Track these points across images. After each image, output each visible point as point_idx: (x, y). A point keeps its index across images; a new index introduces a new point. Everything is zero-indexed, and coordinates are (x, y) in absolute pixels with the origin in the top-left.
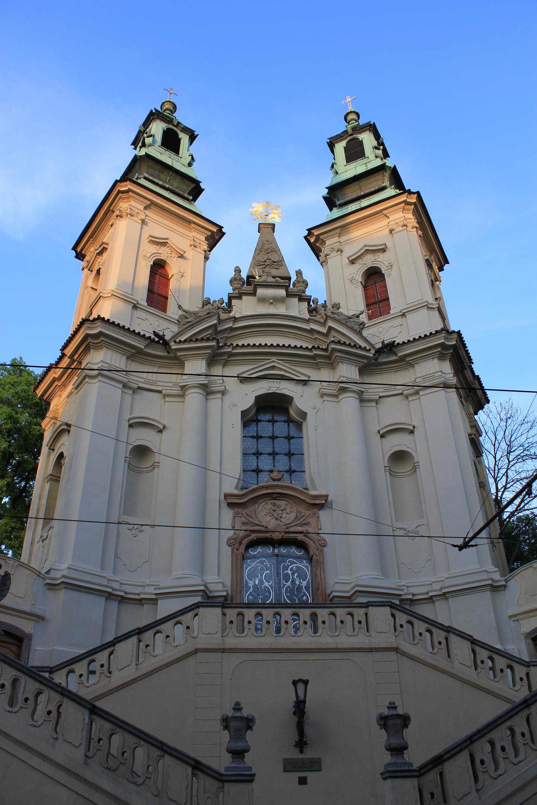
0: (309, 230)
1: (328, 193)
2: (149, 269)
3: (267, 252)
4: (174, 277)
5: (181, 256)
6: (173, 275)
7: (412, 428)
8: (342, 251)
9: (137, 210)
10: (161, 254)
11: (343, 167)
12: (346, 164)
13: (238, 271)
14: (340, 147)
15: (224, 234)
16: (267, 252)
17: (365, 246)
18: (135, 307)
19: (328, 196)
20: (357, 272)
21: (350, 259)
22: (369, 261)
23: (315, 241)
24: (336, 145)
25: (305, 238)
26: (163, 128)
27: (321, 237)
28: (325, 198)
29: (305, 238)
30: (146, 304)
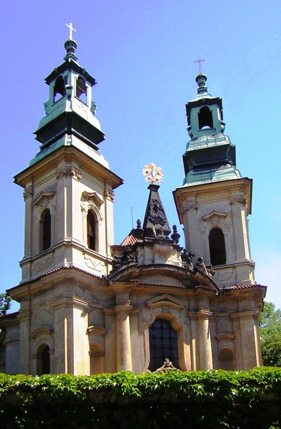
0: (177, 189)
1: (186, 154)
3: (154, 209)
7: (234, 338)
8: (197, 209)
11: (196, 131)
12: (198, 130)
13: (139, 222)
14: (195, 112)
15: (123, 183)
16: (154, 209)
17: (214, 211)
19: (186, 155)
20: (208, 227)
21: (204, 218)
22: (215, 222)
23: (179, 195)
24: (192, 109)
25: (174, 192)
27: (185, 195)
28: (183, 157)
29: (174, 192)
30: (87, 247)
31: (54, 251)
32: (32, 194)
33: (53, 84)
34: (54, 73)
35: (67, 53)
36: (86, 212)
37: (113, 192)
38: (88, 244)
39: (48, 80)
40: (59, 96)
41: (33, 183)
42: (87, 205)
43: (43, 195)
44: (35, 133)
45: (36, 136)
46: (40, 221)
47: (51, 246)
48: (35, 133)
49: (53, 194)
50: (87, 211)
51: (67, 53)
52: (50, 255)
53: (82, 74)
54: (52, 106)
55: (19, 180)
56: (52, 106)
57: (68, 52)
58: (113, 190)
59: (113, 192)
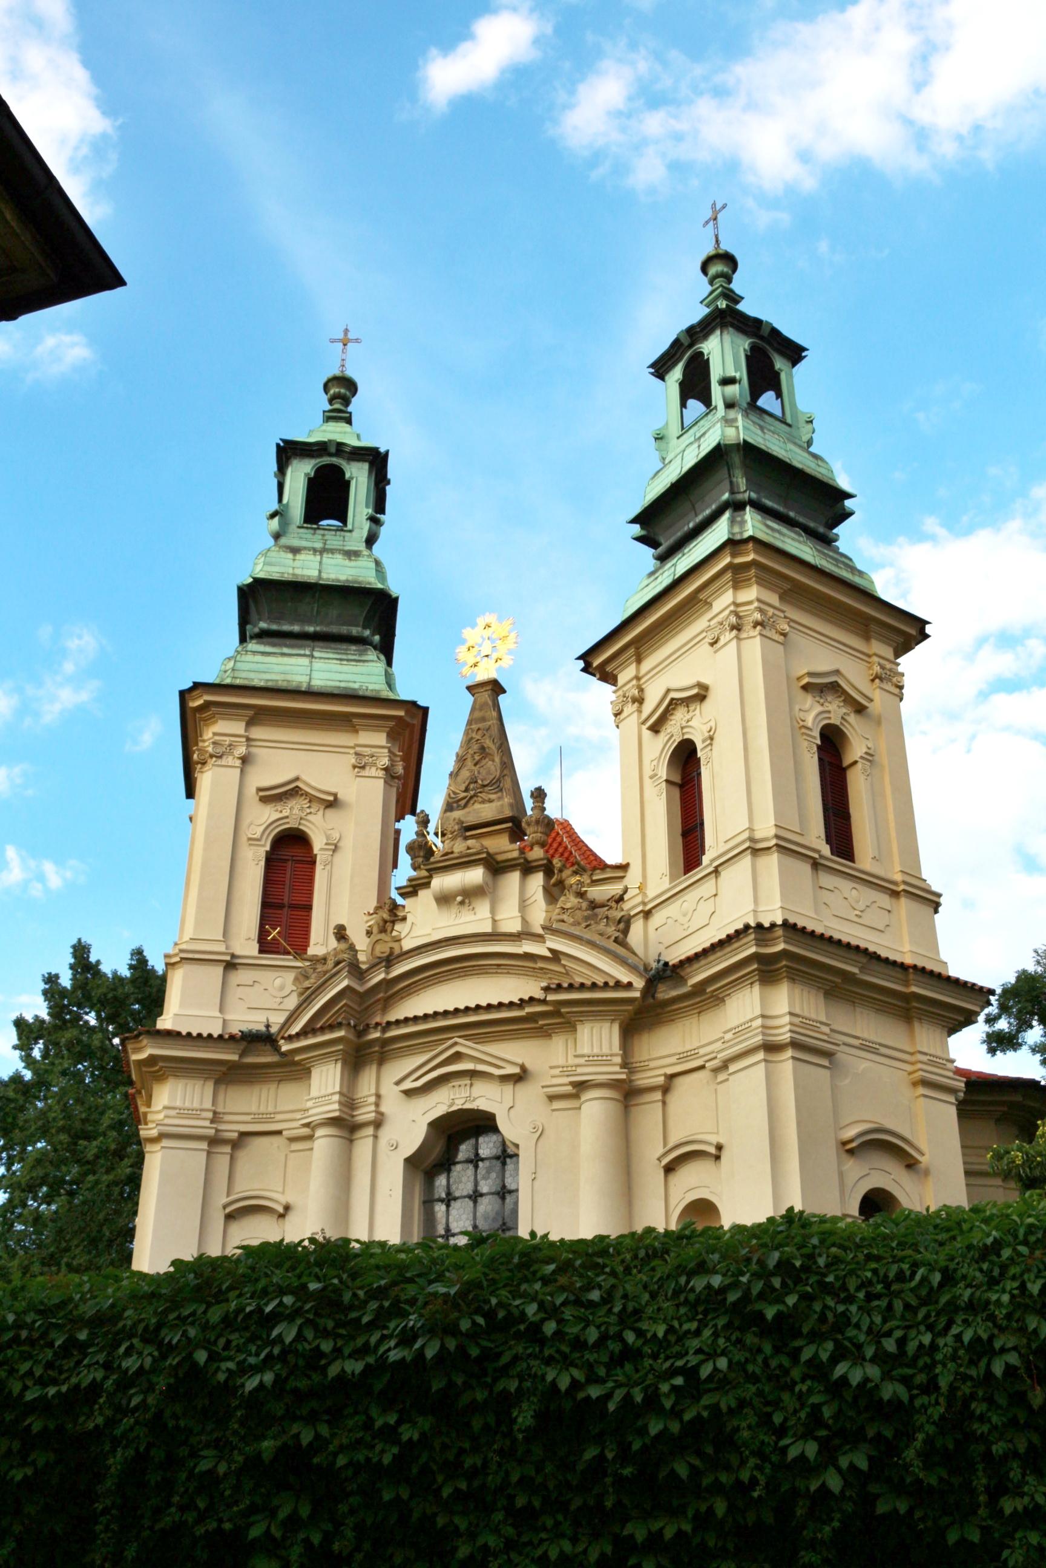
2: (816, 757)
4: (859, 766)
5: (860, 709)
6: (855, 762)
9: (771, 611)
10: (829, 712)
15: (927, 636)
18: (816, 865)
26: (745, 350)
30: (826, 850)
31: (716, 871)
32: (639, 700)
33: (676, 374)
34: (676, 343)
35: (710, 288)
36: (814, 738)
37: (898, 664)
38: (828, 841)
39: (660, 368)
40: (695, 406)
41: (638, 670)
42: (814, 713)
43: (672, 699)
44: (634, 521)
45: (636, 529)
46: (667, 781)
47: (706, 859)
48: (634, 521)
49: (703, 693)
50: (816, 733)
51: (710, 288)
52: (707, 888)
53: (761, 338)
54: (678, 438)
55: (595, 664)
56: (678, 438)
57: (711, 283)
58: (898, 661)
59: (898, 664)
